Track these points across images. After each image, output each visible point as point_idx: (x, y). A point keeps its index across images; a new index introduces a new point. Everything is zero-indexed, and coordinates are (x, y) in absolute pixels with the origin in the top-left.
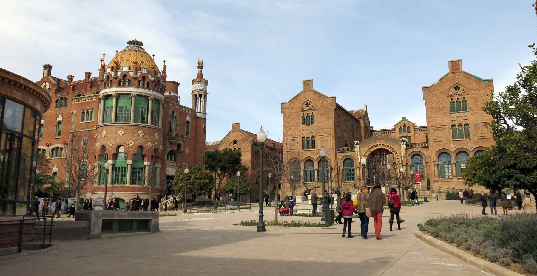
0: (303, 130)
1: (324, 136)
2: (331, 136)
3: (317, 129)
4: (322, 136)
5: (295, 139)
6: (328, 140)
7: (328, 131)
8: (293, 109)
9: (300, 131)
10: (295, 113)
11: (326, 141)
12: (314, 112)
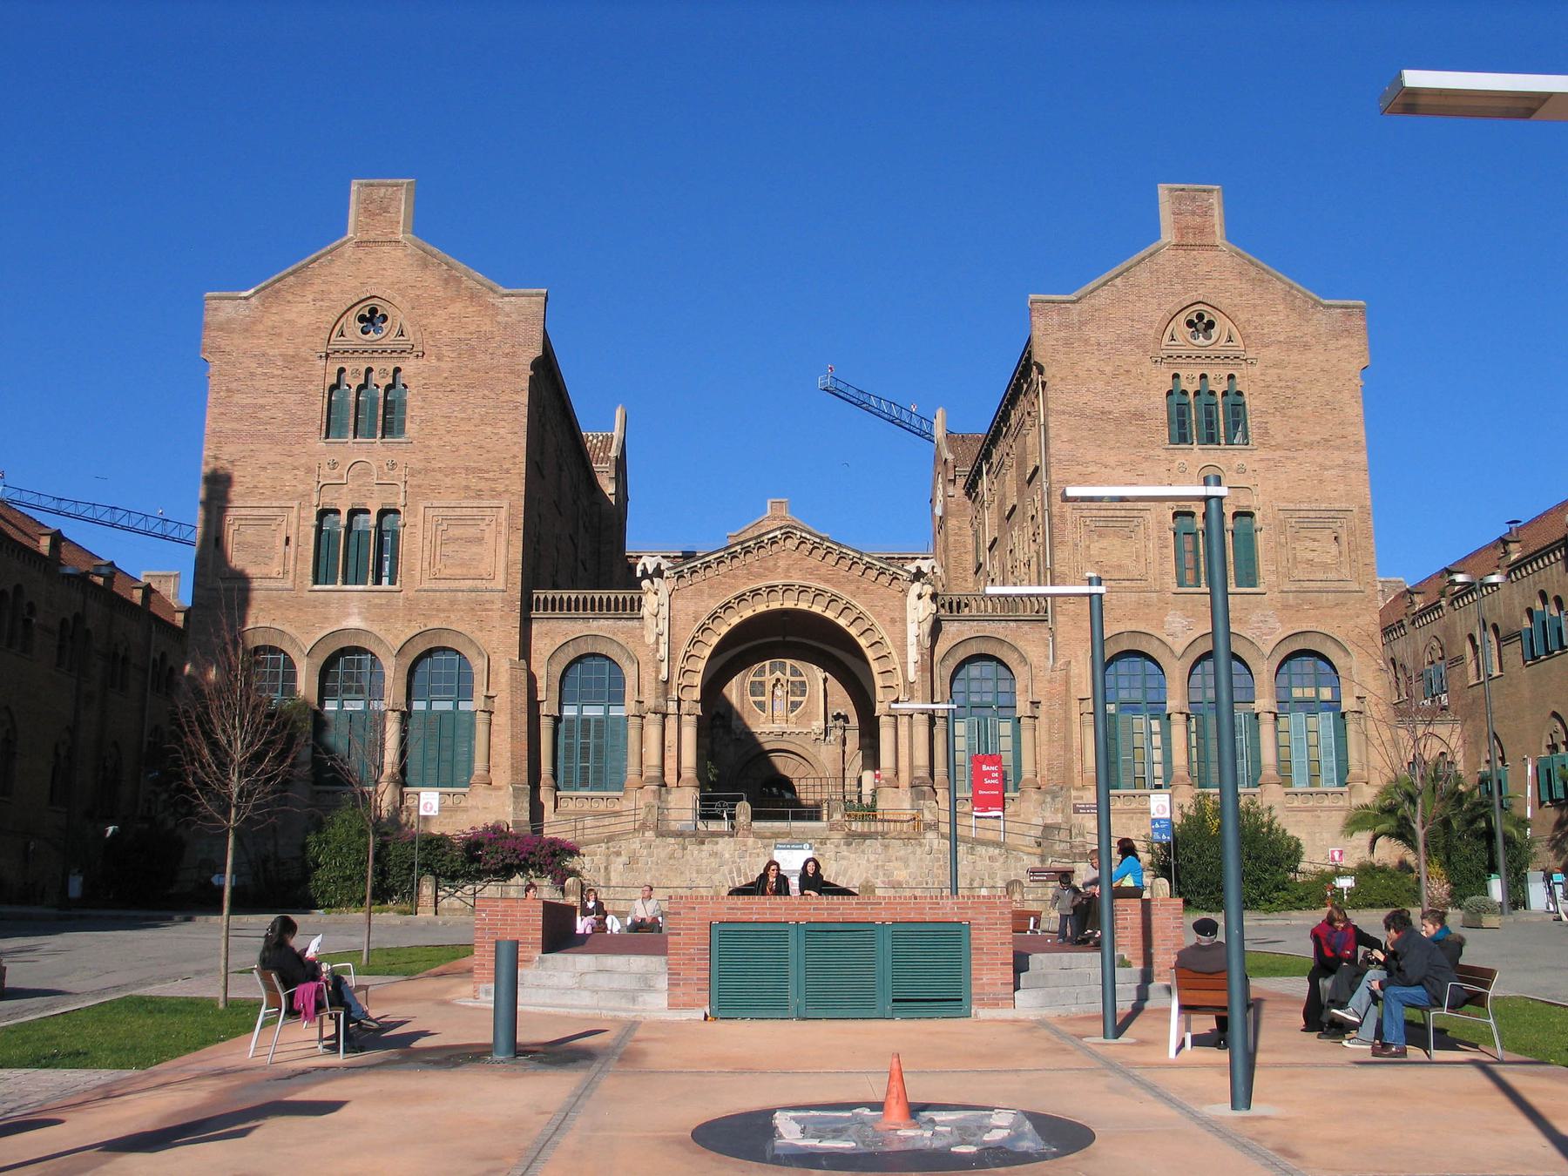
0: (334, 465)
1: (458, 512)
2: (503, 513)
3: (419, 466)
4: (450, 512)
5: (273, 518)
6: (480, 540)
7: (483, 485)
8: (280, 335)
9: (309, 470)
10: (290, 361)
11: (469, 541)
12: (409, 367)
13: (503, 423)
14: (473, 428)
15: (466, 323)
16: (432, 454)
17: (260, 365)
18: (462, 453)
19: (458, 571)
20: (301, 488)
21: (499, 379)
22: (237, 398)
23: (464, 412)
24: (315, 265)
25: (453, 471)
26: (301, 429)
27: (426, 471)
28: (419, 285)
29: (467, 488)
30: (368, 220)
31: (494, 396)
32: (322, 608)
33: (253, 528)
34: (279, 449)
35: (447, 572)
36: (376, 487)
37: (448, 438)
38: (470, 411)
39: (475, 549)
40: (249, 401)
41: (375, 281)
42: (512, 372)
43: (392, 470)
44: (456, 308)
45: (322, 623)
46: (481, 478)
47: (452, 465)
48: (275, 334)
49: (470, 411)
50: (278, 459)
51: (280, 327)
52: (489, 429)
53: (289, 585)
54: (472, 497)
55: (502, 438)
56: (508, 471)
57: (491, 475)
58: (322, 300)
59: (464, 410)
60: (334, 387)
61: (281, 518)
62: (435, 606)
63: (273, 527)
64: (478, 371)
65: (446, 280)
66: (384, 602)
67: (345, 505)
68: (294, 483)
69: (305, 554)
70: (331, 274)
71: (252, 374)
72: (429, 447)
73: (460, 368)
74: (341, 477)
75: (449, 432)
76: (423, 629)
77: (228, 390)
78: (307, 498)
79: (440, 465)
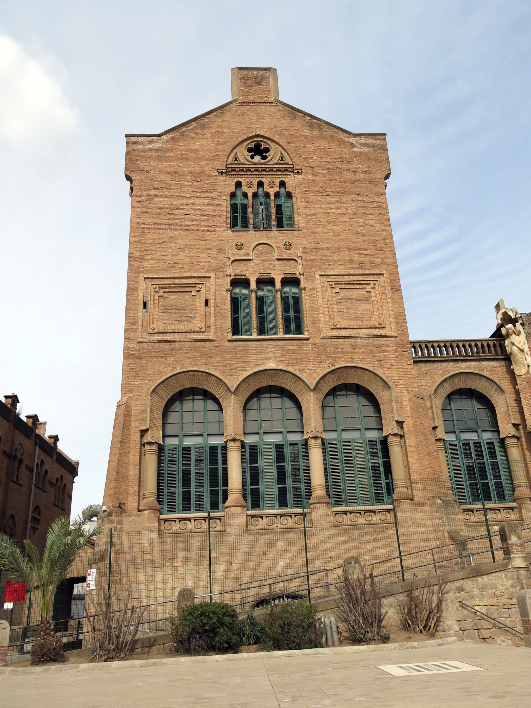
1: (347, 278)
4: (341, 279)
6: (368, 300)
10: (196, 176)
11: (358, 300)
13: (371, 216)
14: (348, 220)
15: (330, 152)
16: (319, 238)
17: (173, 179)
18: (343, 236)
19: (354, 324)
20: (214, 263)
21: (361, 187)
22: (156, 201)
23: (340, 209)
24: (210, 116)
25: (338, 250)
26: (211, 222)
27: (317, 250)
28: (291, 129)
29: (351, 261)
30: (247, 90)
31: (360, 198)
32: (243, 354)
33: (174, 296)
34: (193, 236)
35: (344, 324)
36: (277, 262)
37: (330, 226)
38: (344, 209)
39: (364, 306)
40: (165, 203)
41: (256, 126)
42: (371, 183)
43: (289, 249)
44: (322, 143)
45: (242, 366)
46: (361, 254)
47: (336, 245)
48: (184, 158)
49: (344, 209)
50: (193, 243)
51: (187, 154)
52: (361, 221)
53: (212, 336)
54: (357, 268)
55: (372, 226)
56: (381, 249)
57: (368, 252)
58: (218, 137)
59: (339, 208)
60: (233, 195)
61: (200, 286)
62: (339, 350)
63: (193, 293)
64: (345, 182)
65: (310, 126)
66: (295, 347)
67: (253, 275)
68: (209, 259)
69: (222, 311)
70: (223, 121)
71: (168, 186)
72: (316, 233)
73: (331, 180)
74: (248, 255)
75: (330, 223)
76: (332, 368)
77: (148, 196)
78: (220, 270)
79: (327, 245)
